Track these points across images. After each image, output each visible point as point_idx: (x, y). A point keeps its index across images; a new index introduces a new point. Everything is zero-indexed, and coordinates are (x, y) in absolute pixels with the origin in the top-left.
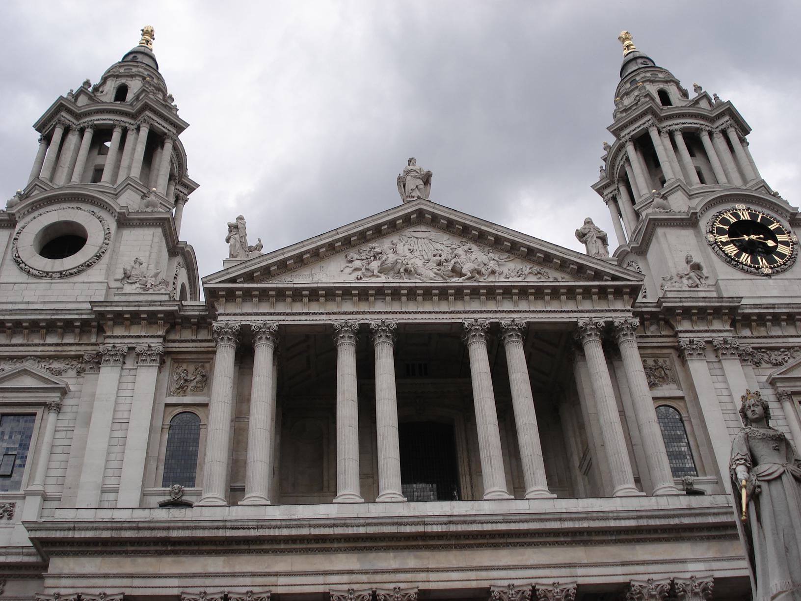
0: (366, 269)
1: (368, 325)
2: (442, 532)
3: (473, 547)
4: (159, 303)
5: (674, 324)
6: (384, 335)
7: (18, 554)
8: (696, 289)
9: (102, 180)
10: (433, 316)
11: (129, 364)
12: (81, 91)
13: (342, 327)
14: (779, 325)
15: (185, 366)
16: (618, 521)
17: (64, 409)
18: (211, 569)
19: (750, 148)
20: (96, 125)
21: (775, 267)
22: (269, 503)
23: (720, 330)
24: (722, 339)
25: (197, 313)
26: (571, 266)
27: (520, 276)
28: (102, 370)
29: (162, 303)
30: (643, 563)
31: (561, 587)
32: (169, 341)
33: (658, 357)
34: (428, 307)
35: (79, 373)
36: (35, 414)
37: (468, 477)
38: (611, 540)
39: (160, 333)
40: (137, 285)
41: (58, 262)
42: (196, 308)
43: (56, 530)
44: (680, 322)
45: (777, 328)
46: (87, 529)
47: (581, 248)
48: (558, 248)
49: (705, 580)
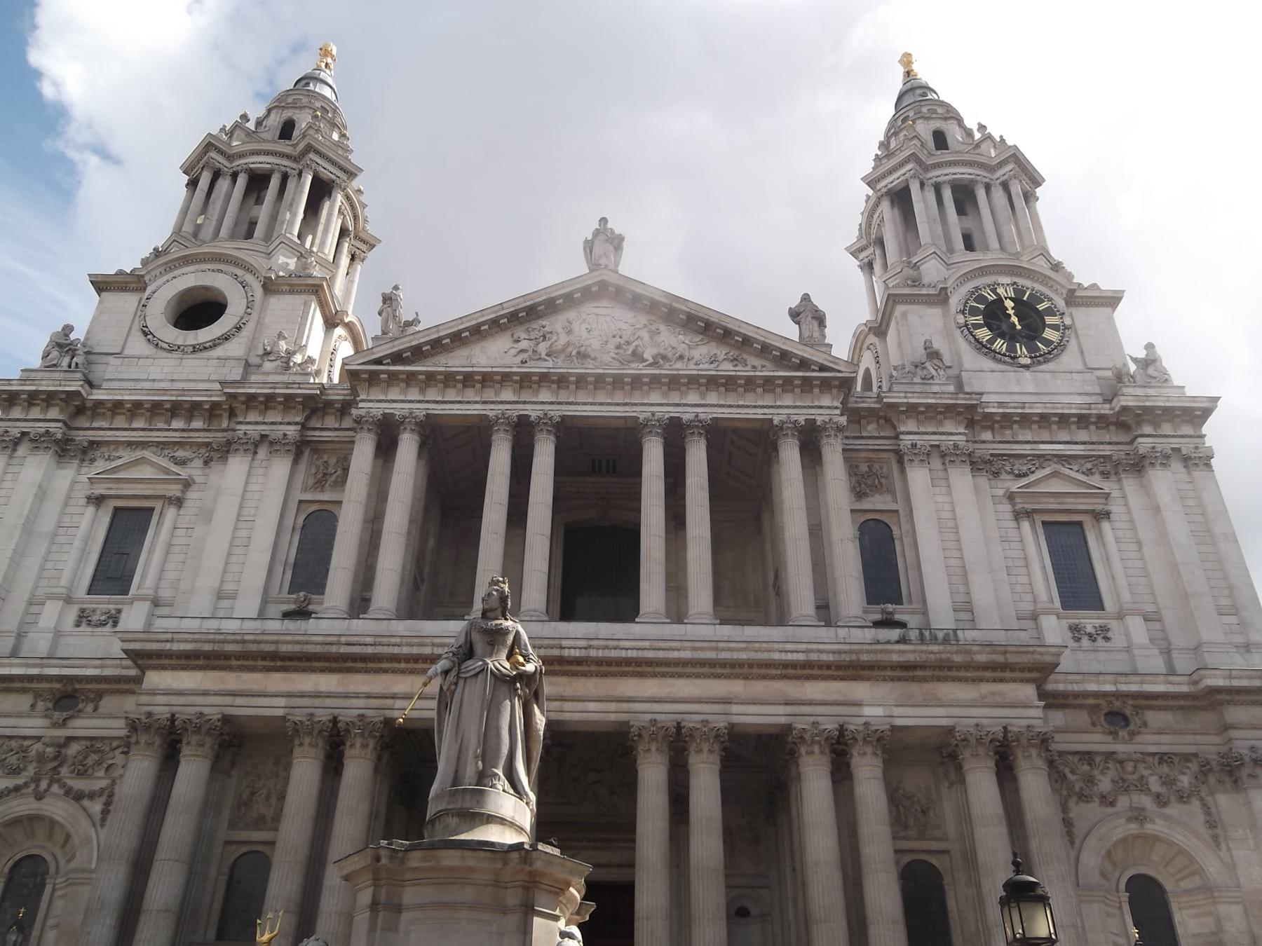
0: (534, 351)
1: (528, 416)
2: (580, 657)
3: (616, 676)
4: (301, 386)
6: (545, 428)
7: (117, 666)
8: (931, 381)
9: (255, 235)
11: (262, 452)
12: (236, 126)
13: (498, 419)
14: (1031, 429)
16: (783, 653)
17: (187, 504)
19: (1040, 206)
20: (251, 169)
21: (1036, 357)
22: (394, 617)
23: (954, 434)
24: (952, 443)
26: (774, 352)
27: (712, 363)
28: (230, 458)
29: (301, 386)
30: (811, 703)
31: (711, 726)
32: (310, 429)
33: (874, 462)
34: (601, 397)
35: (206, 463)
36: (152, 509)
38: (776, 675)
39: (298, 419)
40: (278, 362)
41: (191, 334)
42: (340, 392)
43: (153, 641)
45: (1027, 431)
46: (186, 641)
47: (791, 331)
48: (759, 331)
49: (882, 728)
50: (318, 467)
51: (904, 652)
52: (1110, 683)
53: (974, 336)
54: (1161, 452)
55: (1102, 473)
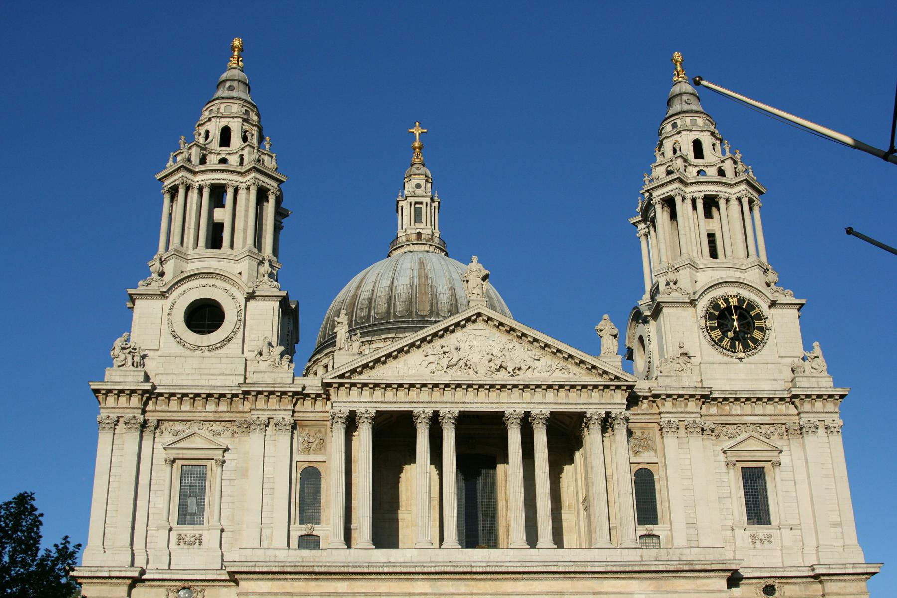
5: (660, 405)
7: (214, 574)
8: (682, 373)
10: (484, 405)
15: (307, 430)
16: (593, 567)
18: (340, 591)
20: (212, 184)
21: (747, 351)
24: (692, 419)
25: (315, 392)
27: (549, 371)
33: (645, 429)
37: (504, 502)
41: (205, 337)
42: (314, 388)
44: (663, 404)
50: (304, 437)
51: (658, 565)
52: (767, 572)
53: (710, 336)
54: (813, 423)
55: (779, 435)
